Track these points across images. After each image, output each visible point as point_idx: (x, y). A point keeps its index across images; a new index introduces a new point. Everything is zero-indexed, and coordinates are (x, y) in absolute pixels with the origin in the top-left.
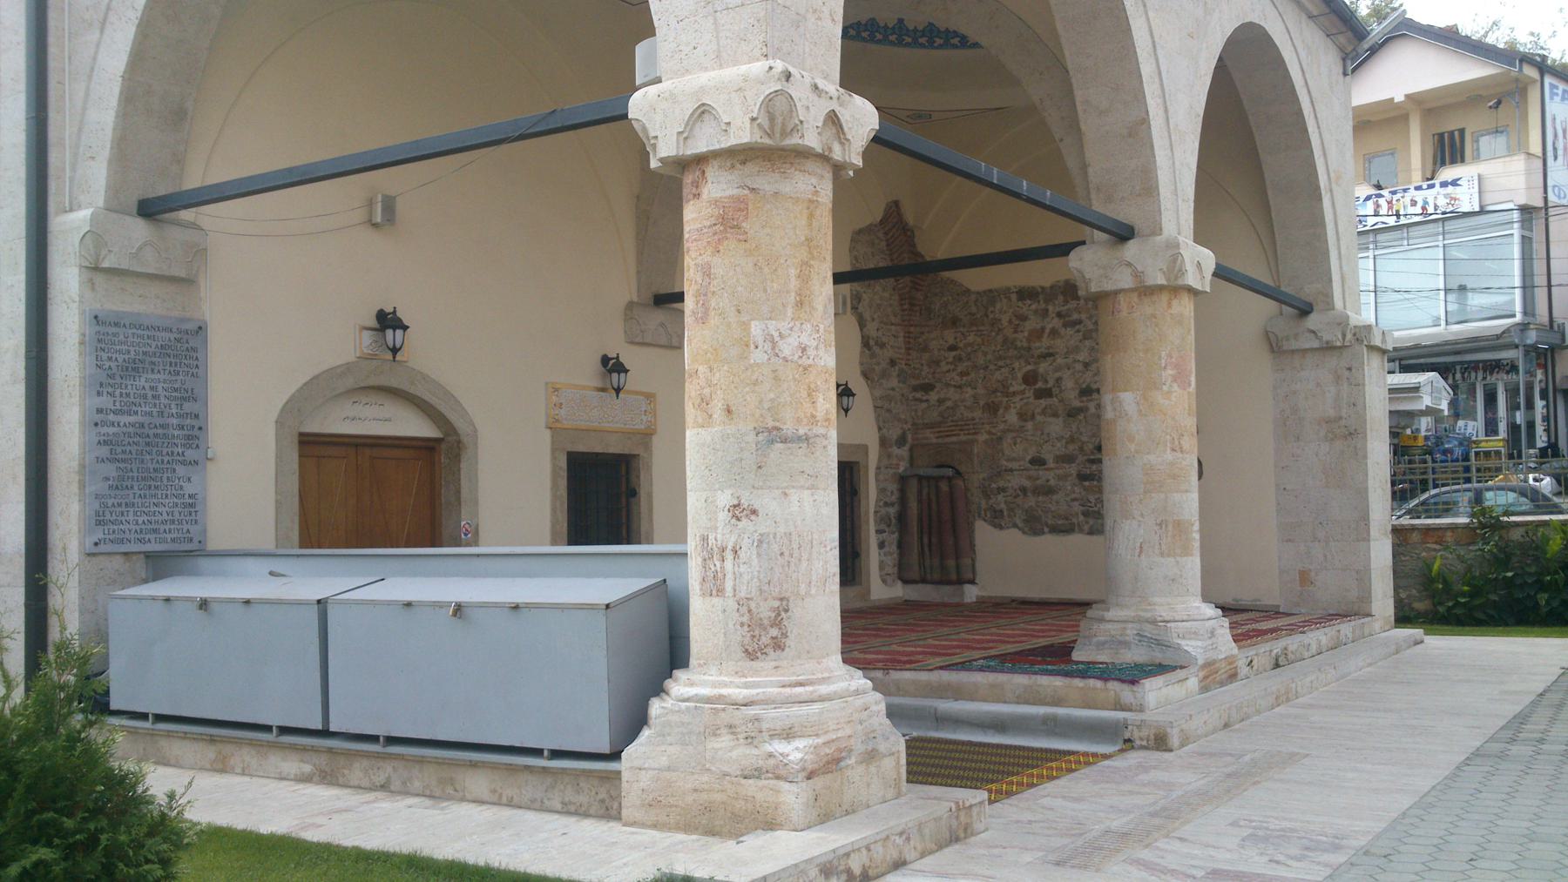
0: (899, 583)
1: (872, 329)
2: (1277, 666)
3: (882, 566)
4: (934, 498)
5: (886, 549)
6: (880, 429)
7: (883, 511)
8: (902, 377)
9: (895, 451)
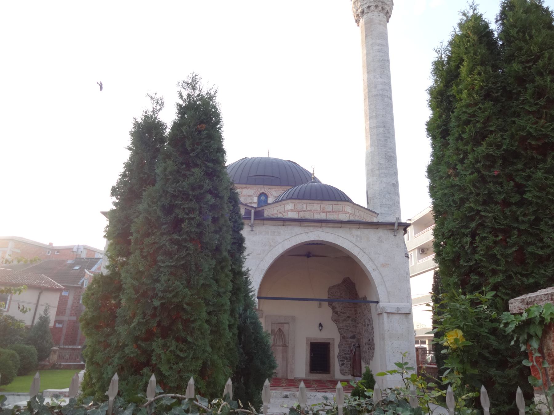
0: (350, 376)
1: (339, 309)
2: (286, 397)
3: (341, 370)
4: (357, 353)
6: (341, 334)
7: (344, 355)
8: (354, 320)
9: (350, 340)
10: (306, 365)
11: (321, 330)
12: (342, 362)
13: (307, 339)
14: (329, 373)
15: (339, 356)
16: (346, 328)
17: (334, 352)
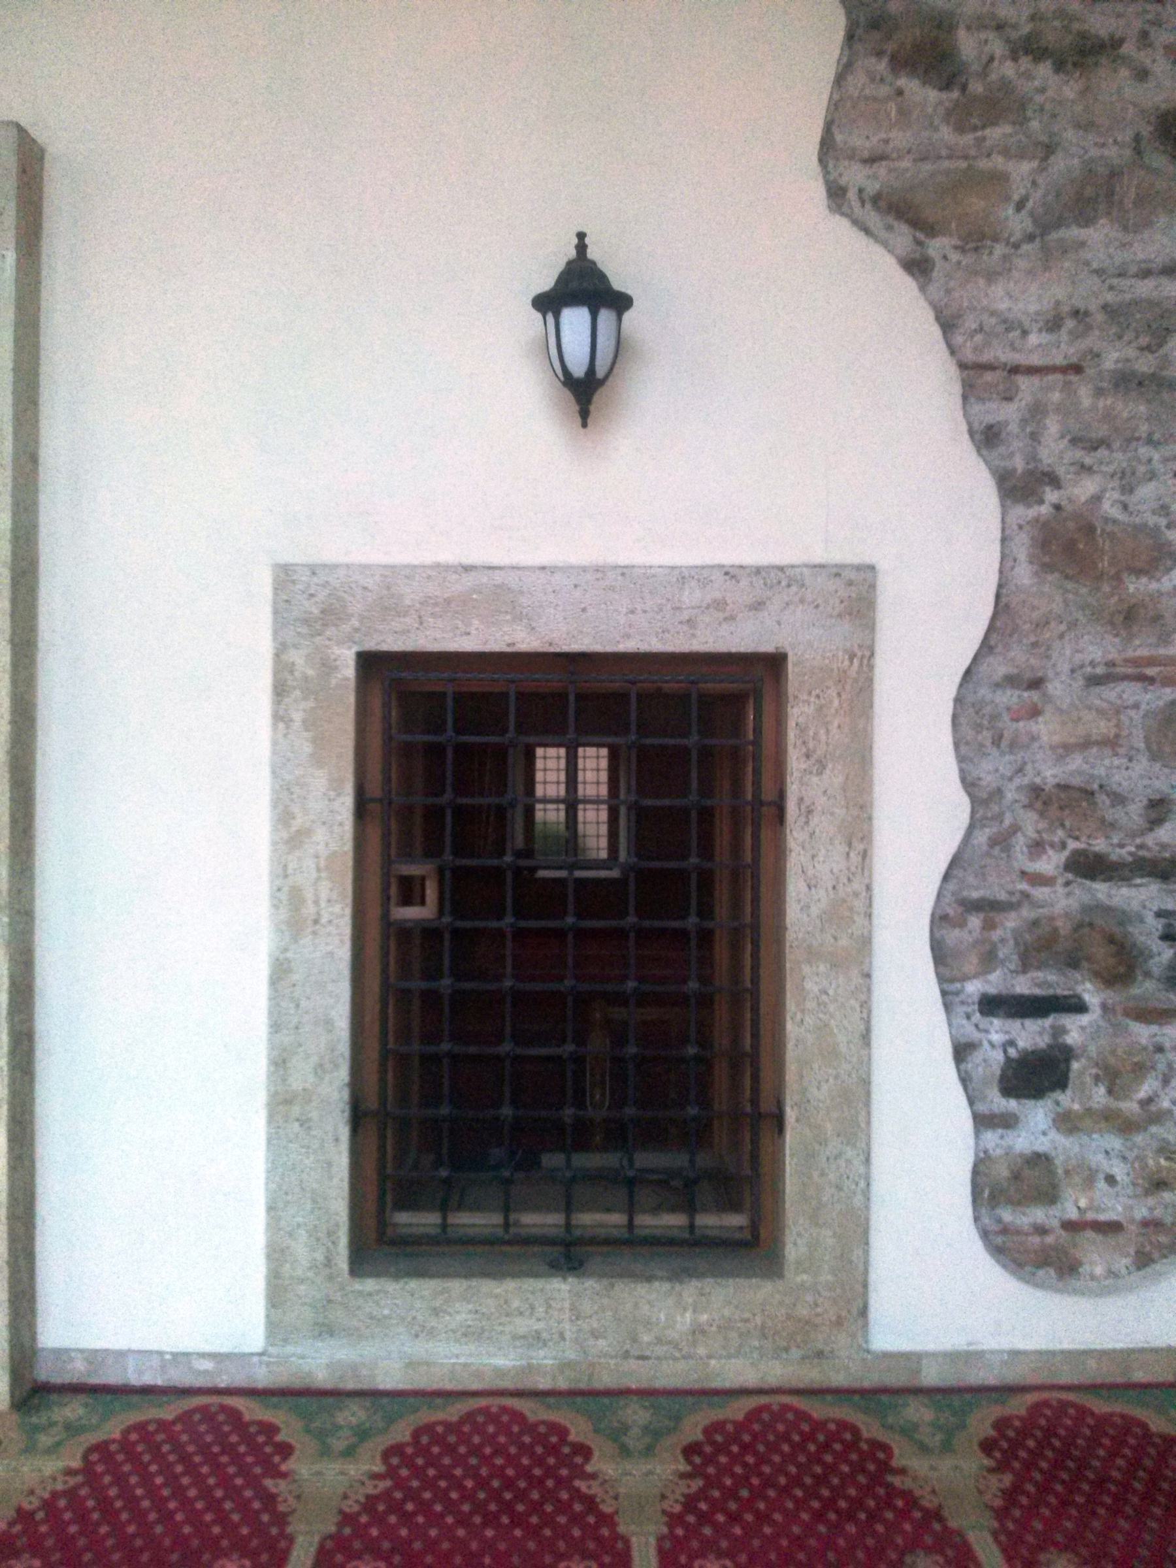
5: (1086, 1092)
6: (1016, 487)
7: (1063, 900)
10: (283, 1104)
11: (584, 393)
12: (1030, 1035)
13: (304, 600)
14: (753, 1247)
15: (964, 912)
16: (1111, 359)
17: (858, 834)
